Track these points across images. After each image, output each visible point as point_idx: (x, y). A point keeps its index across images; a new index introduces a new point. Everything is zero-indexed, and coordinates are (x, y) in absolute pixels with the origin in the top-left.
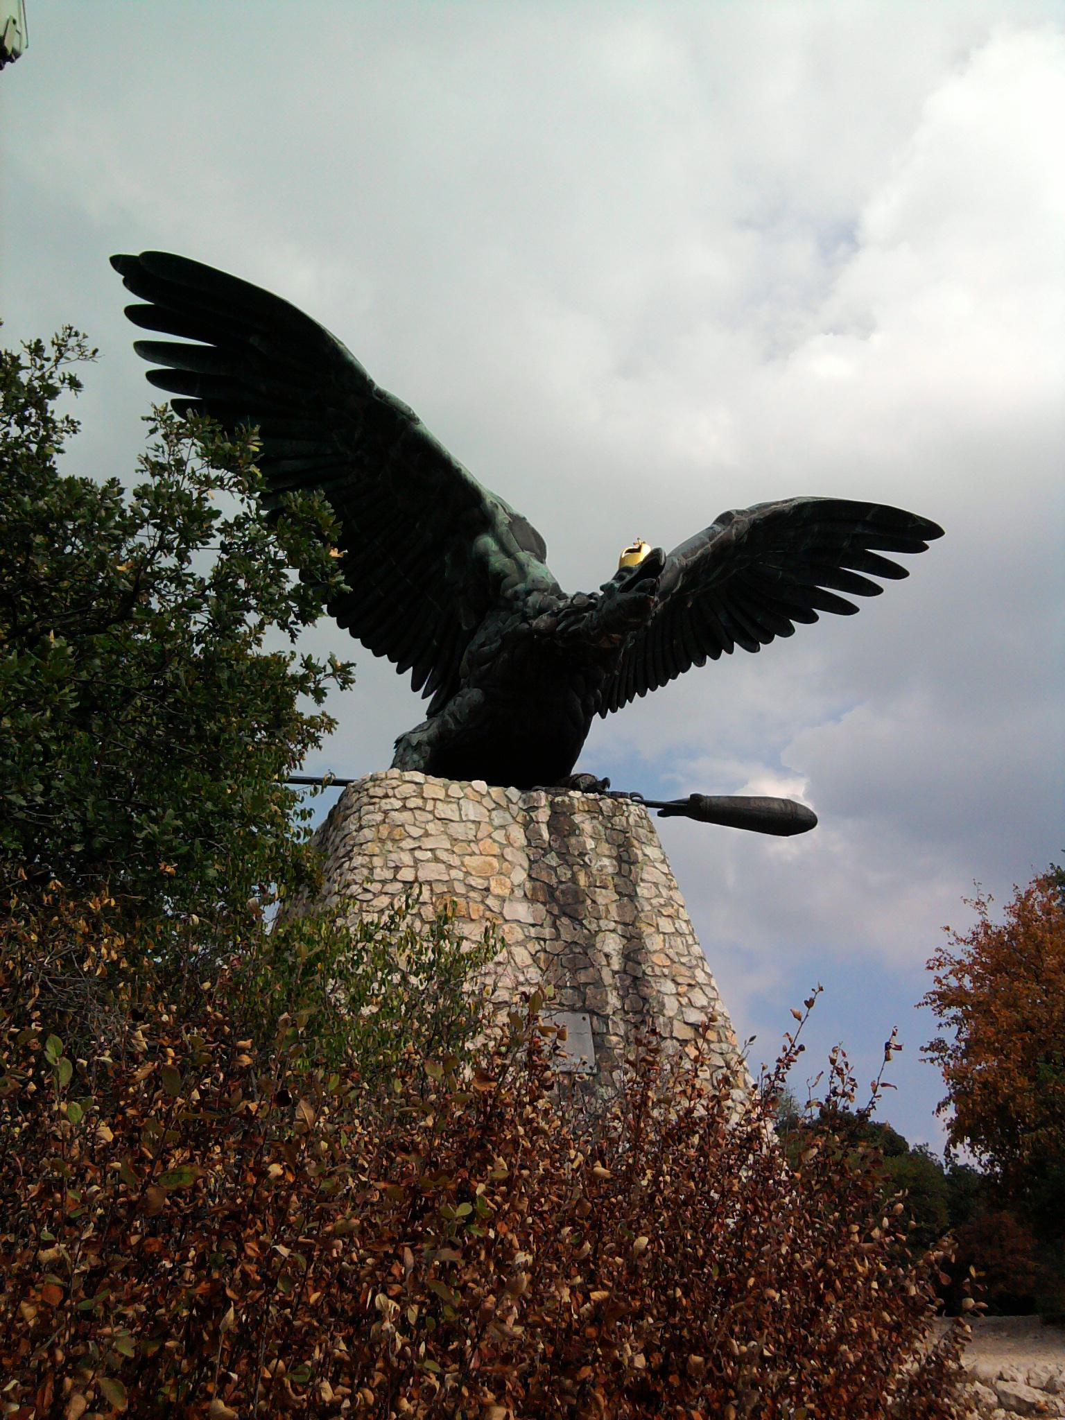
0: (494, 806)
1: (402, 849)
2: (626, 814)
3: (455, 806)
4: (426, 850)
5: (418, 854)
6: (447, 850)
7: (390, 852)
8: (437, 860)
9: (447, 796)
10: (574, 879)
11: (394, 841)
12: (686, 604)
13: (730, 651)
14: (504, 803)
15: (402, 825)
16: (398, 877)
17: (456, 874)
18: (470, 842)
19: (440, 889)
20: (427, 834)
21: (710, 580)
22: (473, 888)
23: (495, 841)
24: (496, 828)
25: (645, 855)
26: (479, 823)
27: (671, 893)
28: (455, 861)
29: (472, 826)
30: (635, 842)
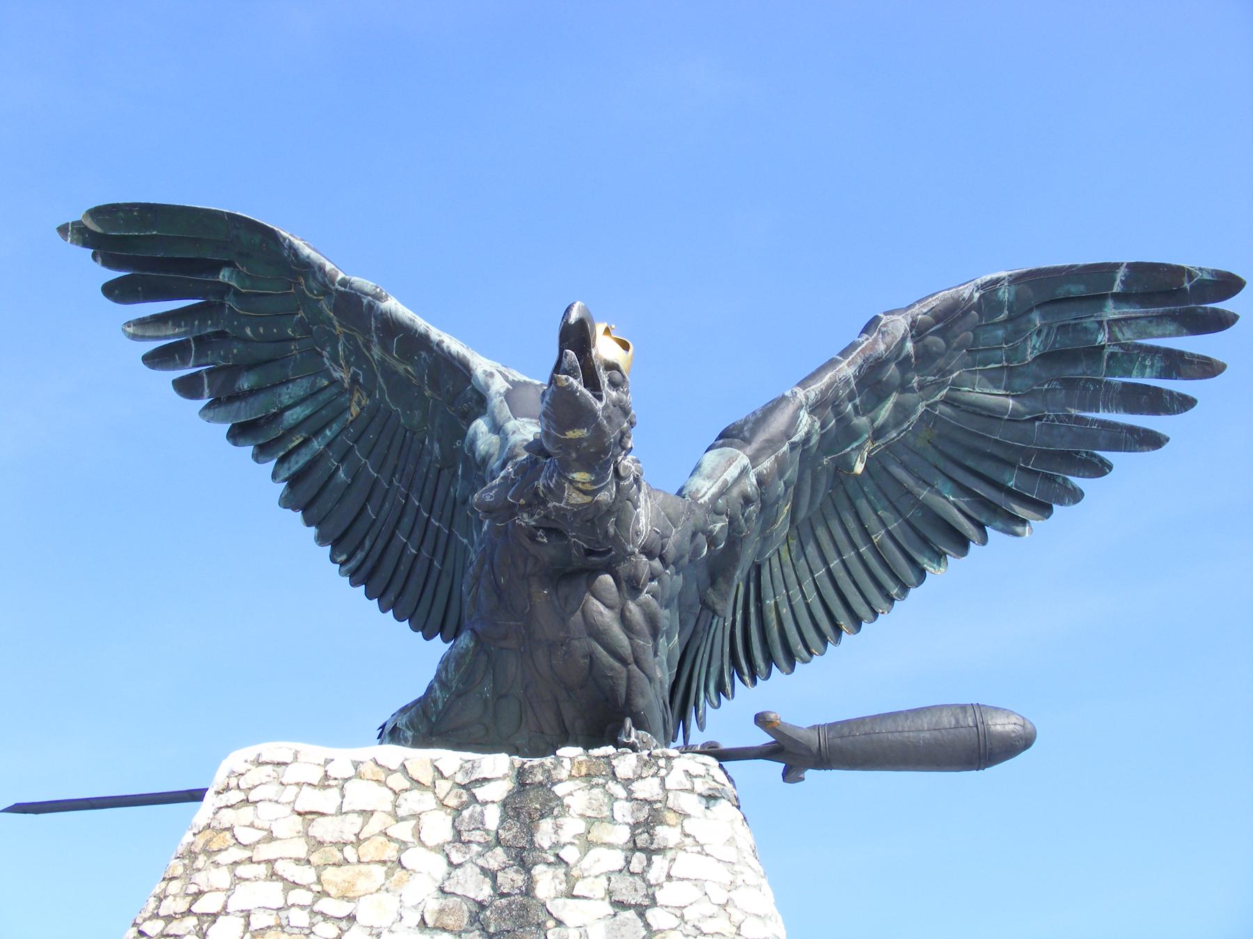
0: (407, 784)
1: (217, 865)
2: (663, 772)
3: (335, 792)
4: (259, 863)
5: (242, 871)
6: (298, 861)
7: (199, 870)
8: (273, 875)
9: (326, 776)
10: (528, 891)
11: (209, 853)
12: (852, 468)
13: (984, 540)
14: (426, 779)
15: (230, 829)
16: (194, 909)
17: (298, 896)
18: (345, 844)
19: (258, 922)
20: (270, 838)
21: (880, 421)
22: (326, 917)
23: (390, 839)
24: (403, 819)
25: (687, 835)
26: (372, 812)
27: (733, 895)
28: (306, 875)
29: (359, 820)
30: (670, 817)
